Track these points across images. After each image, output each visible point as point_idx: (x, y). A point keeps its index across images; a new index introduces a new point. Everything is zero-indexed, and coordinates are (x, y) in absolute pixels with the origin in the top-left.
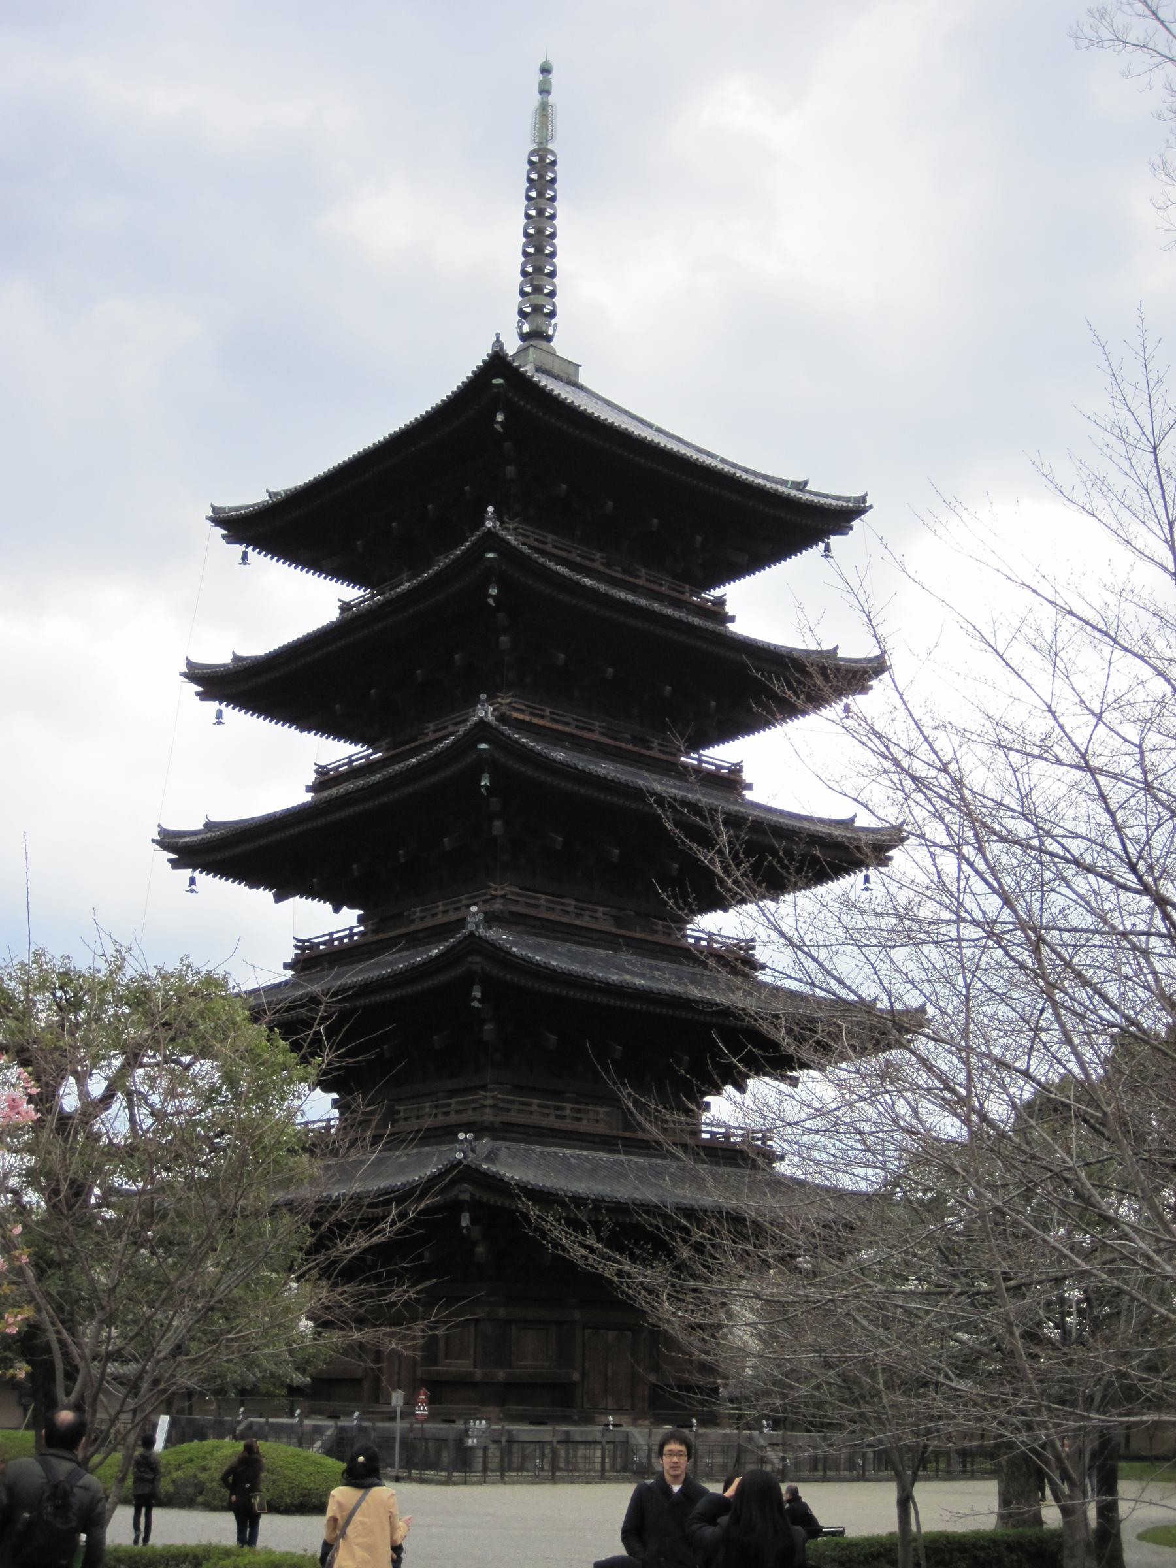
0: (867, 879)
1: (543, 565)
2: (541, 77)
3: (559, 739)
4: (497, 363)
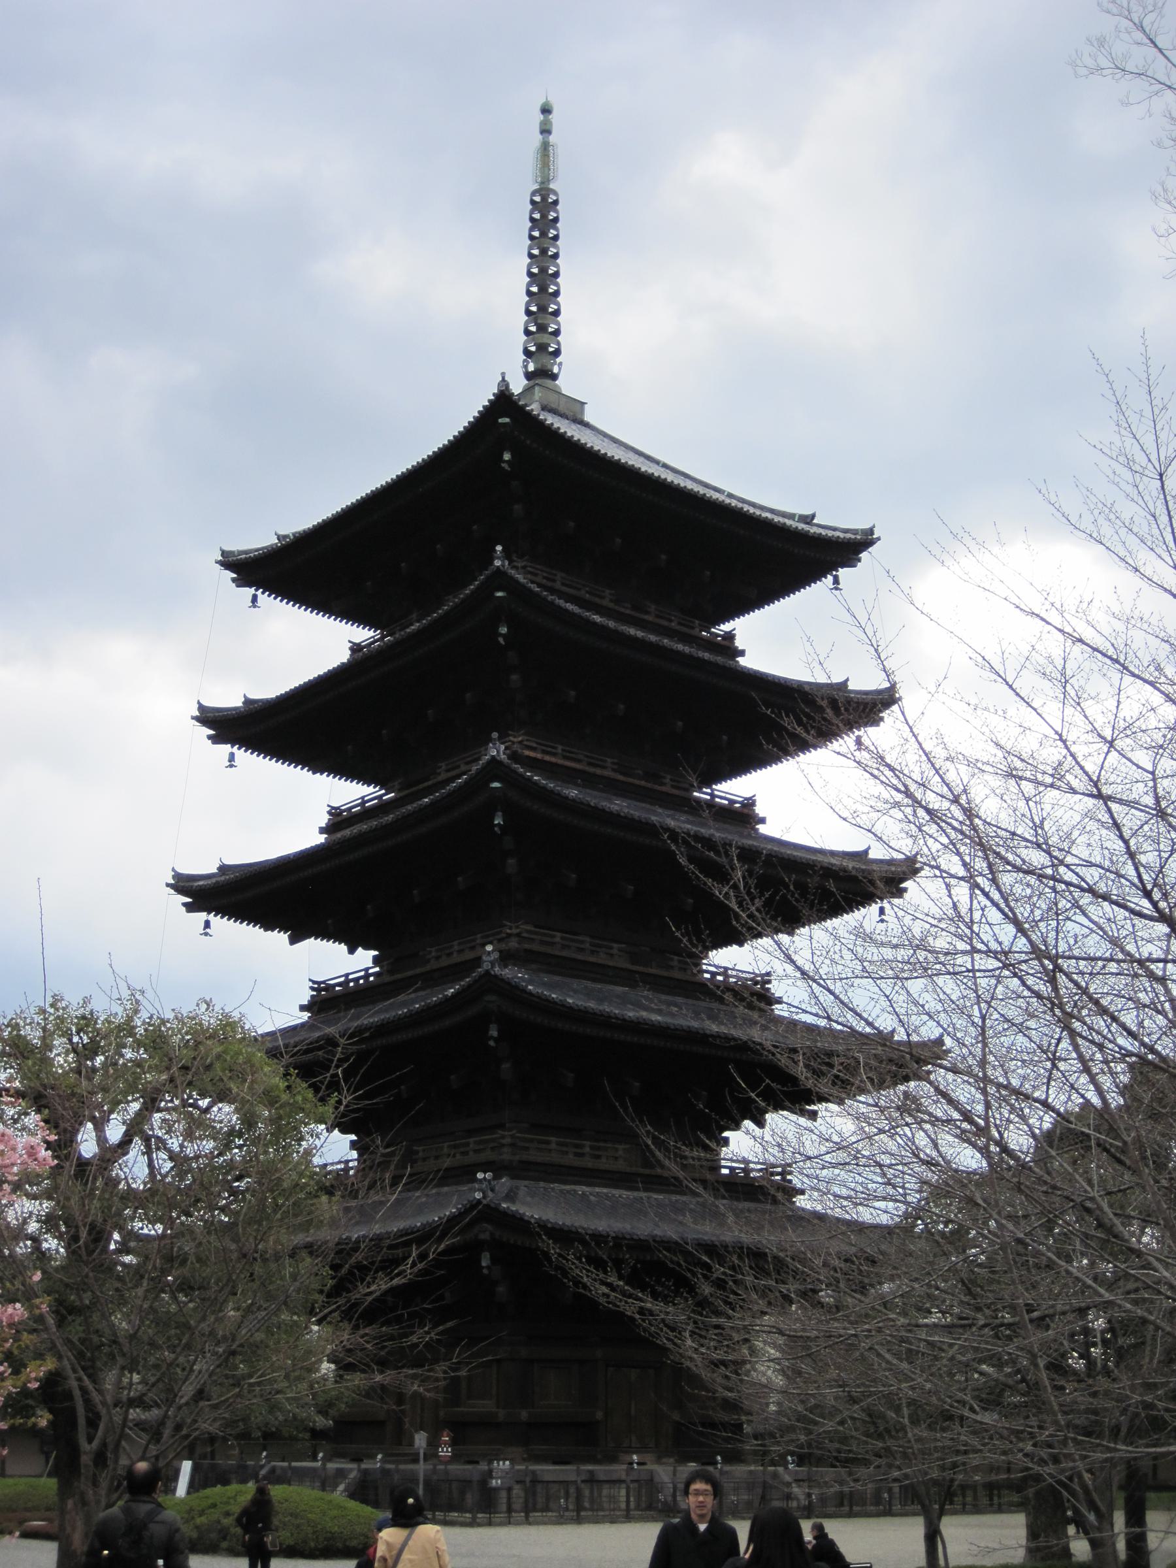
0: (882, 911)
1: (552, 603)
2: (542, 117)
3: (570, 776)
4: (503, 401)
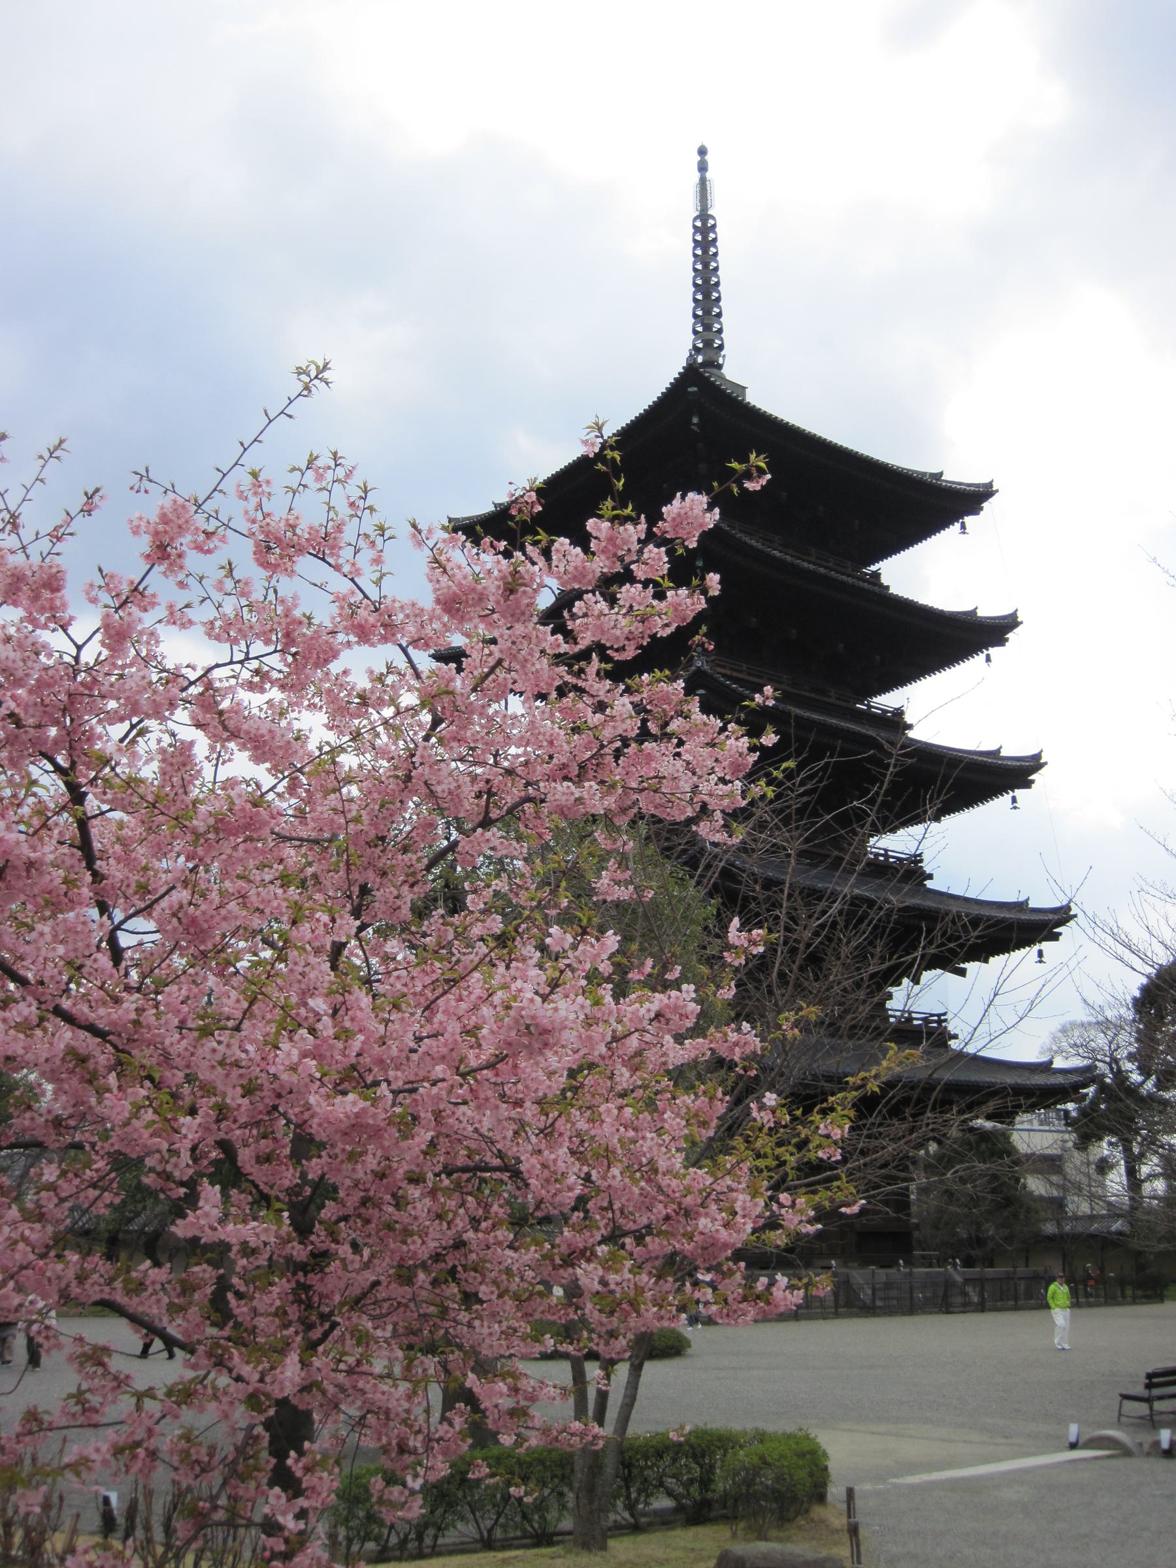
0: (1014, 800)
1: (739, 540)
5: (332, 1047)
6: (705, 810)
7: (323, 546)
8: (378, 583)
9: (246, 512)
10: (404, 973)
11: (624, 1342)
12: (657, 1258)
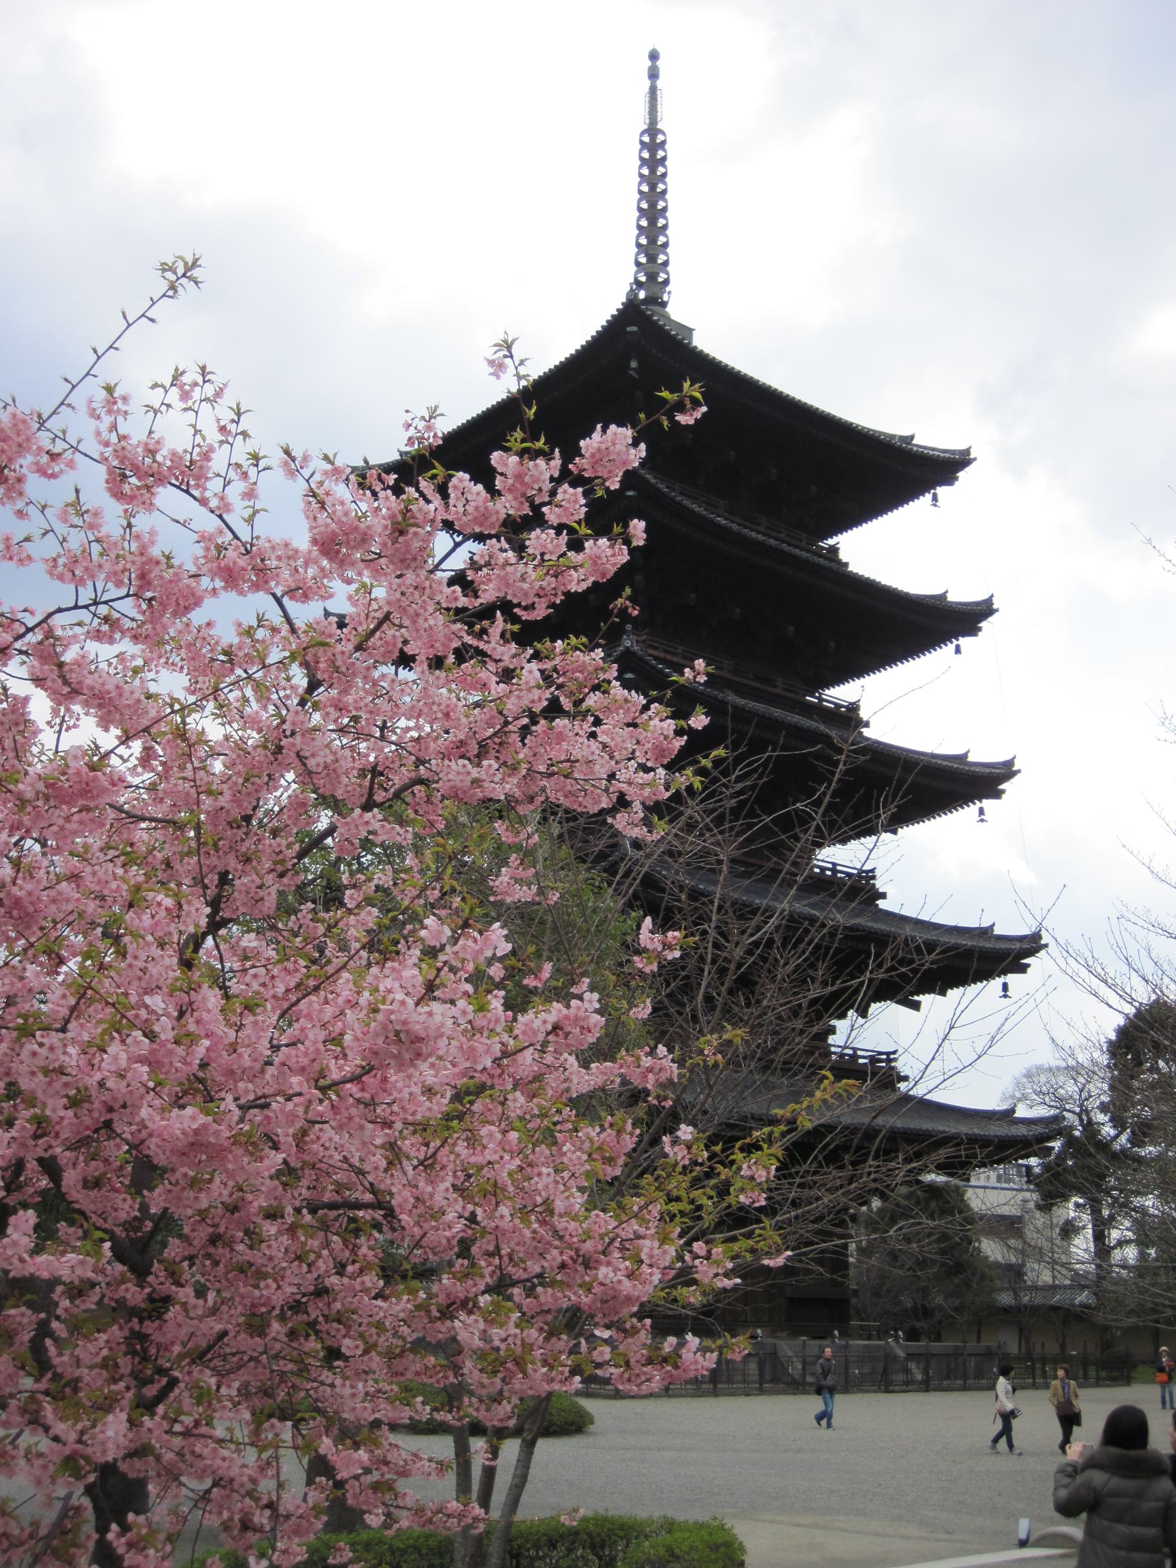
0: (981, 811)
1: (679, 503)
5: (171, 1053)
6: (623, 802)
7: (188, 474)
8: (250, 520)
9: (98, 433)
10: (262, 971)
11: (509, 1408)
12: (548, 1311)
